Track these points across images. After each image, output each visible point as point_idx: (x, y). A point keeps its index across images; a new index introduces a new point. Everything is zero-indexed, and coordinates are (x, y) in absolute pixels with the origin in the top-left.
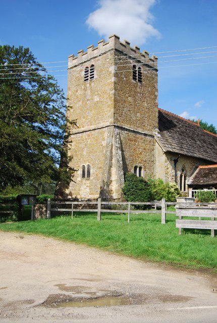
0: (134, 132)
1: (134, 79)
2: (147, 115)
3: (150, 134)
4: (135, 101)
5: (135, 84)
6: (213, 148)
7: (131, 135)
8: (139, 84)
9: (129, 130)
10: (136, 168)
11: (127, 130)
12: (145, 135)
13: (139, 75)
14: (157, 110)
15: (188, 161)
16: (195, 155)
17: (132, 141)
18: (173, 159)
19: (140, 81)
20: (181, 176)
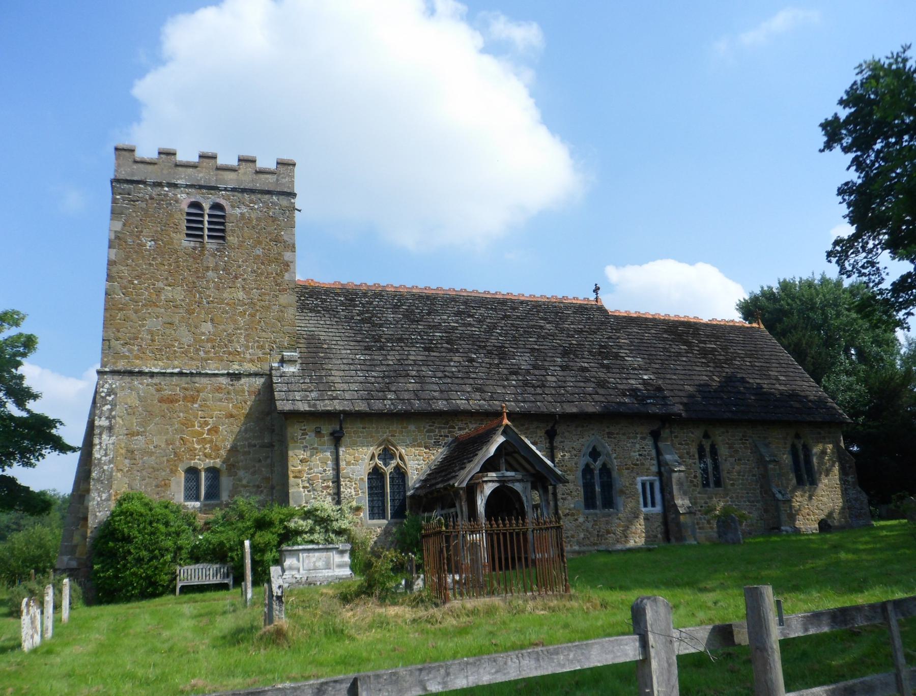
0: (181, 374)
1: (194, 231)
2: (241, 322)
3: (253, 368)
4: (192, 288)
5: (194, 248)
6: (603, 366)
7: (174, 387)
8: (211, 245)
9: (164, 374)
10: (193, 472)
11: (152, 375)
12: (236, 376)
13: (210, 223)
14: (288, 299)
15: (412, 427)
16: (441, 405)
17: (177, 401)
18: (326, 429)
19: (218, 233)
20: (376, 475)
